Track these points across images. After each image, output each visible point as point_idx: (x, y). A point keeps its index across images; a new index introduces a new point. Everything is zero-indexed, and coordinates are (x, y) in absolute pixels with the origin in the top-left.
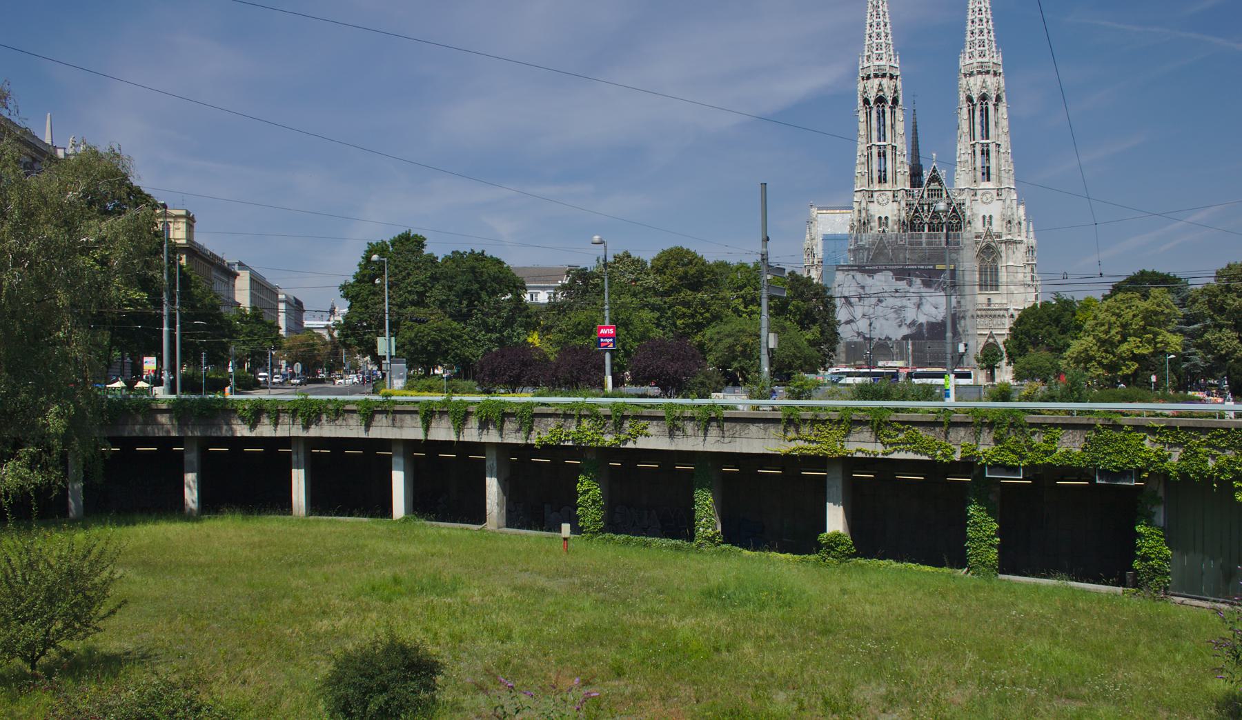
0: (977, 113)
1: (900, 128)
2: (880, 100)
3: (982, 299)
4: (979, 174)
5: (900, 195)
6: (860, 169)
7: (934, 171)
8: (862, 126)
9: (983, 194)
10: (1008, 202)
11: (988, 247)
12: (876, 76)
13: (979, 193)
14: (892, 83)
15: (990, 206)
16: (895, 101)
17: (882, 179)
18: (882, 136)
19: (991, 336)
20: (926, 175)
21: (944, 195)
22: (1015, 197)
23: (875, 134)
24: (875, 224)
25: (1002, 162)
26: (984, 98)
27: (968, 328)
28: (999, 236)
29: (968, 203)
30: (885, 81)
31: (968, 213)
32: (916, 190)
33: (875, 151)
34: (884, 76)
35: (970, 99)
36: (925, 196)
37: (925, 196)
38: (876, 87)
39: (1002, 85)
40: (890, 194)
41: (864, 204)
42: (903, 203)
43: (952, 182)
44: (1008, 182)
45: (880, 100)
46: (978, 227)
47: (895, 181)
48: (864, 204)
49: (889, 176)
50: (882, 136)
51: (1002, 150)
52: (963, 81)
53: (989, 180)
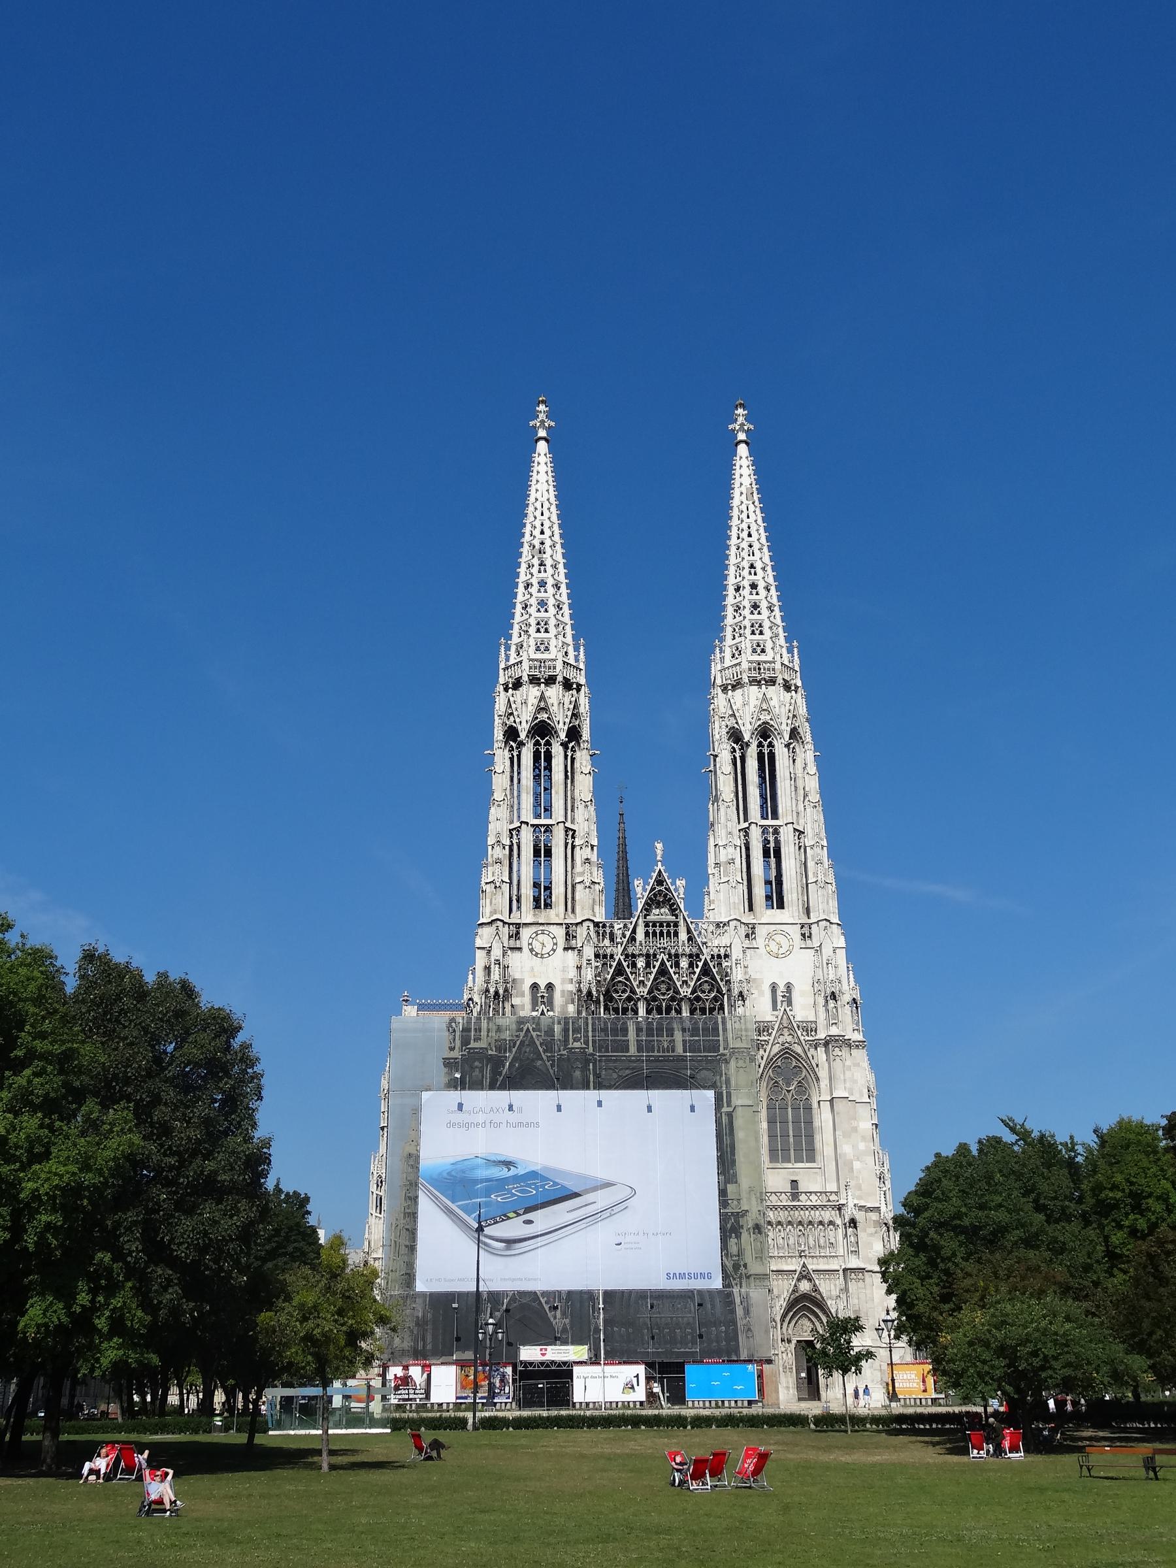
0: (752, 765)
1: (584, 786)
2: (542, 730)
3: (776, 1179)
4: (760, 891)
5: (581, 932)
6: (493, 873)
7: (660, 882)
8: (500, 783)
9: (769, 937)
10: (827, 951)
11: (787, 1053)
12: (534, 680)
13: (761, 931)
14: (568, 697)
15: (786, 964)
16: (574, 733)
17: (542, 901)
18: (543, 806)
19: (805, 1275)
20: (641, 890)
21: (683, 936)
22: (842, 942)
23: (527, 801)
24: (522, 1002)
25: (810, 867)
26: (764, 732)
27: (748, 1258)
28: (809, 1028)
29: (736, 953)
30: (554, 693)
31: (737, 975)
32: (618, 926)
33: (527, 837)
34: (551, 681)
35: (735, 736)
36: (640, 935)
37: (640, 935)
38: (533, 701)
39: (802, 710)
40: (560, 932)
41: (497, 953)
42: (589, 952)
43: (697, 910)
44: (826, 904)
45: (542, 730)
46: (760, 1008)
47: (570, 904)
48: (497, 953)
49: (558, 891)
50: (543, 806)
51: (809, 841)
52: (720, 701)
53: (781, 905)
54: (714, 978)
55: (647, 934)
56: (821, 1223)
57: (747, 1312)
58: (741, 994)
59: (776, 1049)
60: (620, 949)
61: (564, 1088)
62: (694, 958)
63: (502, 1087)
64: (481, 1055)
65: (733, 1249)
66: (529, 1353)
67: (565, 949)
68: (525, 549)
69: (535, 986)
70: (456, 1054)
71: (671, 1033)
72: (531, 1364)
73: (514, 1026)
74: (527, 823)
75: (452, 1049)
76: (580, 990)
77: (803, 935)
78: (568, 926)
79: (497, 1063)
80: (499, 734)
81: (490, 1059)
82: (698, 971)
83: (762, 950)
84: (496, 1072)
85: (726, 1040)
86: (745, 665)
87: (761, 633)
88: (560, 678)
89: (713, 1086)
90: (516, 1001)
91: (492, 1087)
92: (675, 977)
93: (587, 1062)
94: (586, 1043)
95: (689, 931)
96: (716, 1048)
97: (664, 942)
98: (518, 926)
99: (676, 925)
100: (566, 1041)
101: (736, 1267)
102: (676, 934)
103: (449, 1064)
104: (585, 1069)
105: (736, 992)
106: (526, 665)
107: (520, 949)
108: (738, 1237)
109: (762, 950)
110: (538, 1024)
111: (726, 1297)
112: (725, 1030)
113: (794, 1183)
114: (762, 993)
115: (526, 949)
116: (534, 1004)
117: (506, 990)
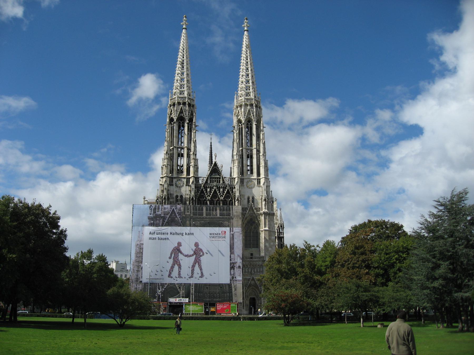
2: (181, 119)
5: (191, 180)
13: (245, 181)
21: (221, 182)
26: (249, 121)
29: (237, 187)
31: (237, 194)
37: (209, 182)
40: (185, 180)
42: (193, 186)
48: (166, 186)
53: (252, 173)
54: (230, 194)
55: (211, 181)
56: (259, 265)
57: (235, 290)
58: (238, 199)
59: (248, 215)
60: (202, 185)
61: (184, 226)
62: (224, 188)
63: (166, 226)
64: (159, 216)
65: (232, 273)
66: (172, 300)
67: (186, 185)
68: (178, 62)
69: (177, 196)
70: (152, 216)
71: (216, 210)
72: (172, 303)
73: (169, 208)
74: (176, 147)
75: (151, 214)
76: (190, 197)
77: (258, 182)
78: (187, 178)
79: (164, 218)
80: (168, 120)
81: (161, 217)
82: (225, 192)
83: (245, 186)
84: (164, 221)
85: (232, 213)
86: (243, 100)
87: (249, 90)
88: (187, 103)
89: (228, 226)
90: (171, 200)
91: (162, 226)
92: (219, 194)
93: (191, 218)
94: (191, 213)
95: (223, 180)
96: (229, 215)
97: (215, 184)
98: (172, 178)
99: (220, 178)
100: (185, 212)
101: (233, 278)
102: (220, 181)
103: (150, 218)
104: (190, 220)
105: (236, 199)
106: (176, 99)
107: (173, 185)
108: (234, 269)
109: (245, 186)
110: (177, 207)
111: (230, 285)
112: (232, 210)
113: (252, 254)
114: (245, 199)
115: (174, 185)
116: (177, 201)
117: (168, 197)
